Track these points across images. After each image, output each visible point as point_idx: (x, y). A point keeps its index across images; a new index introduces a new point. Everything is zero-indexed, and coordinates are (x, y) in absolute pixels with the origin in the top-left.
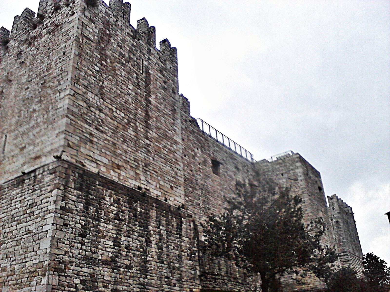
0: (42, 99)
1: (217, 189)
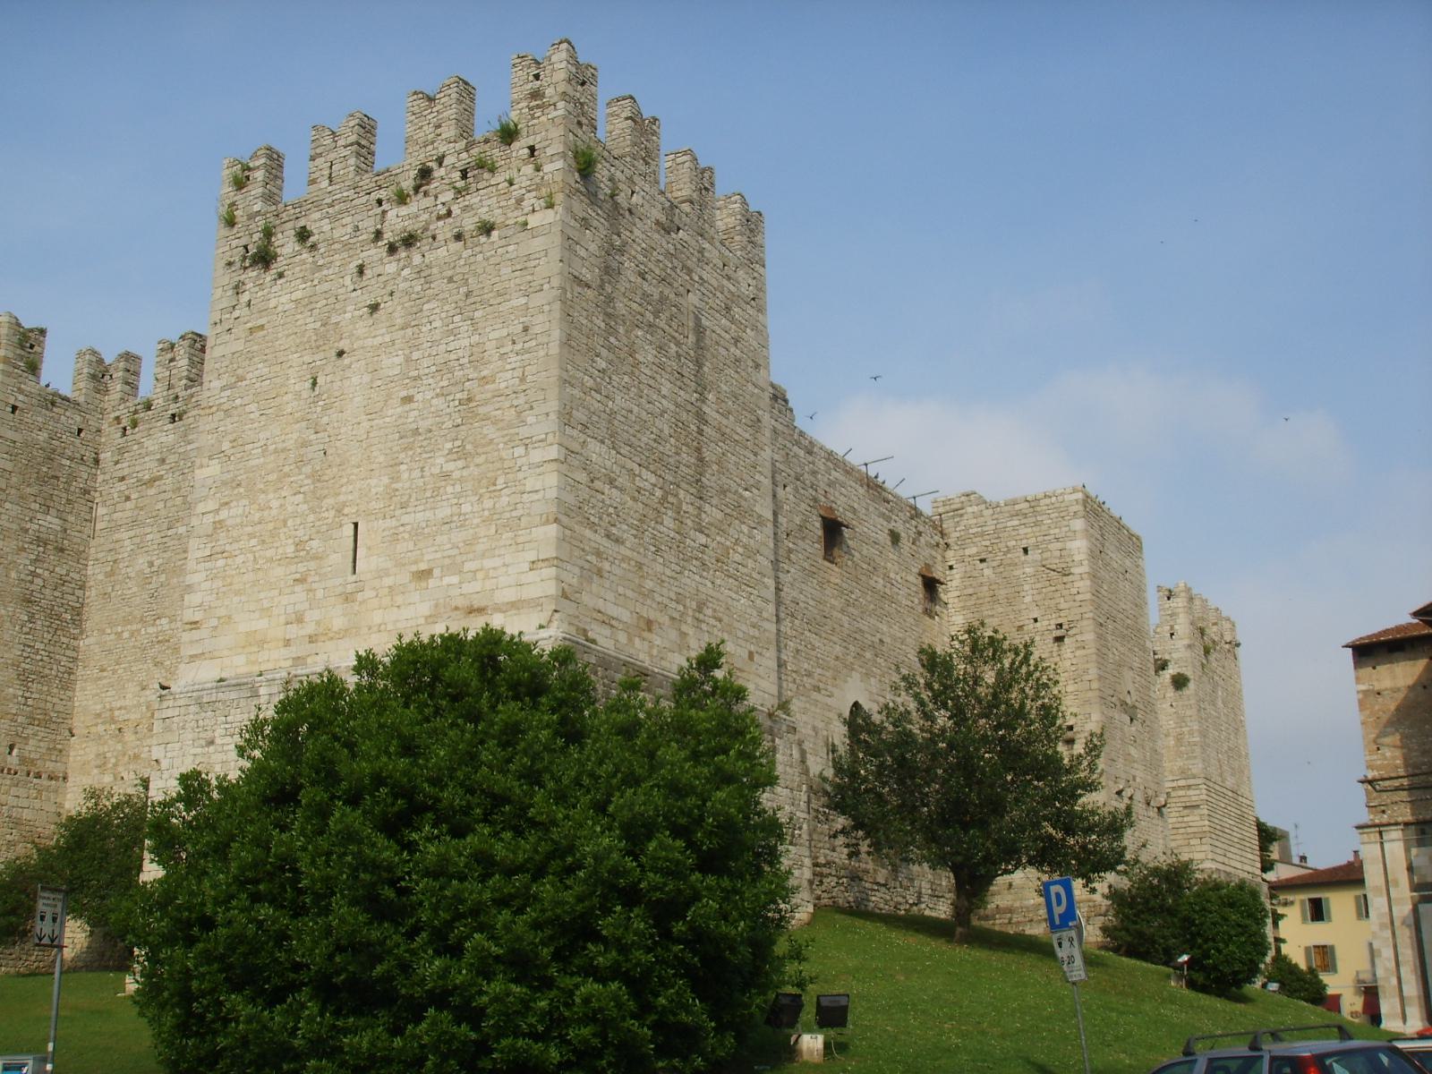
0: (469, 447)
1: (832, 607)
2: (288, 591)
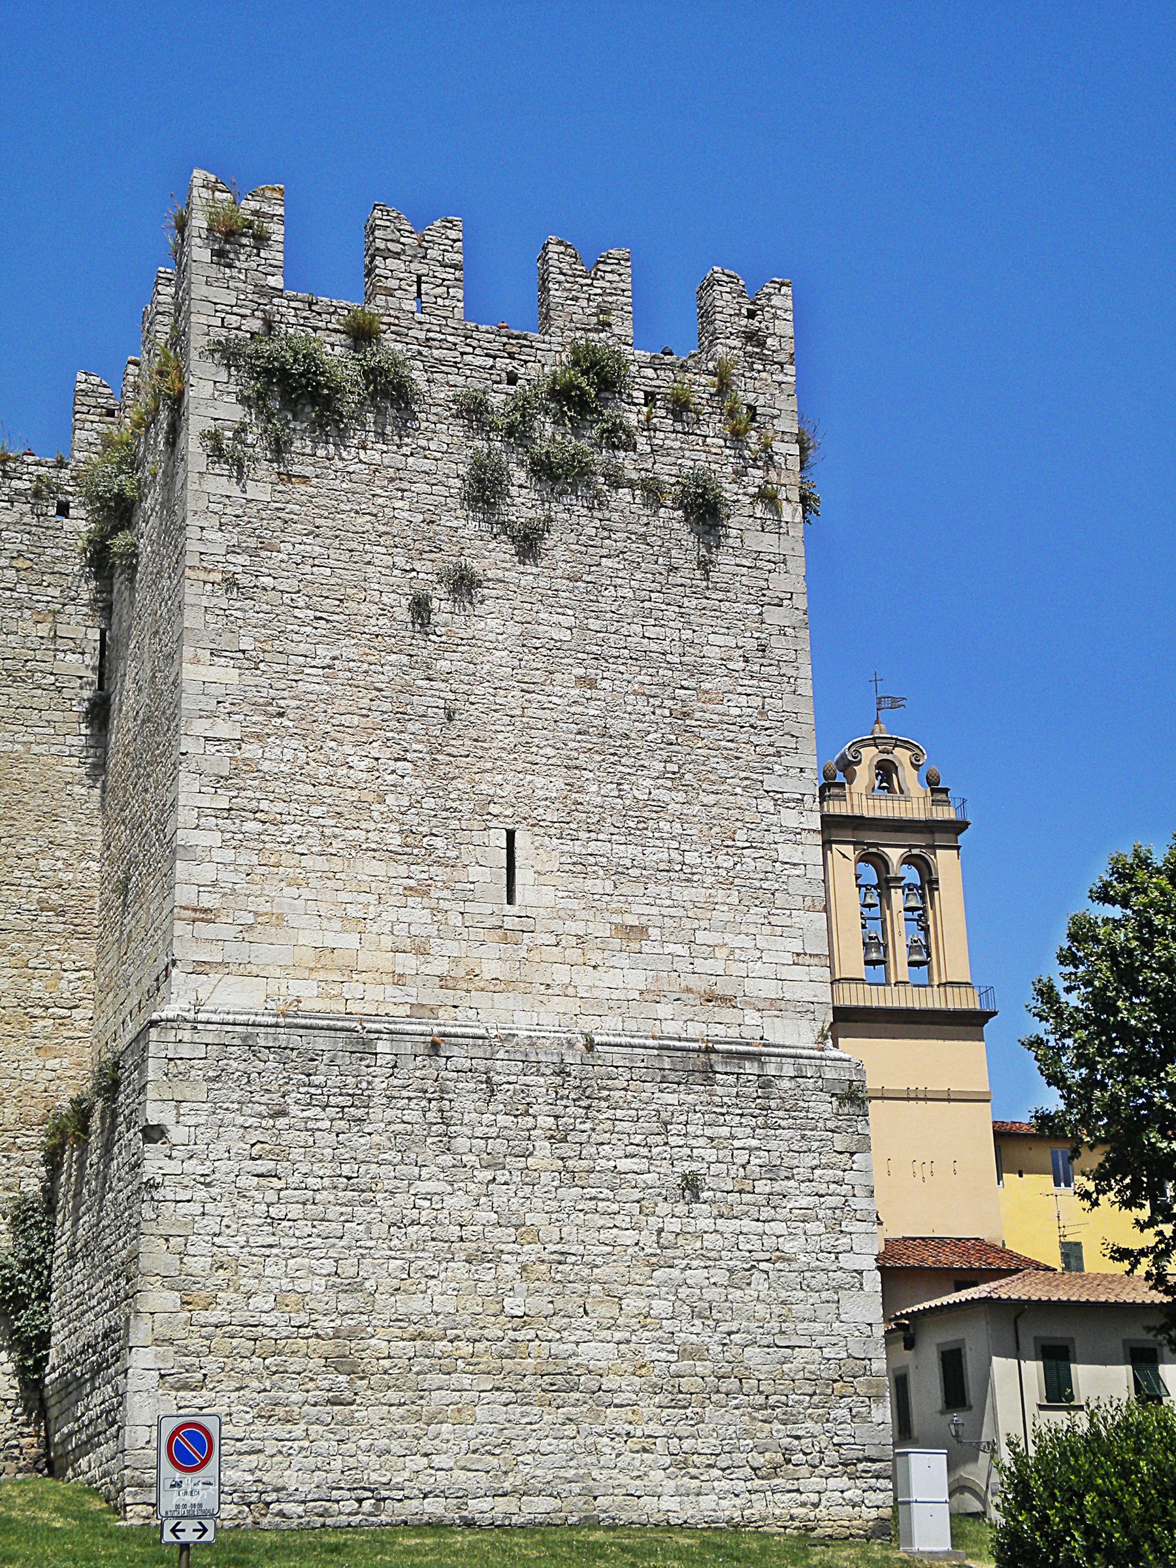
2: (393, 900)
